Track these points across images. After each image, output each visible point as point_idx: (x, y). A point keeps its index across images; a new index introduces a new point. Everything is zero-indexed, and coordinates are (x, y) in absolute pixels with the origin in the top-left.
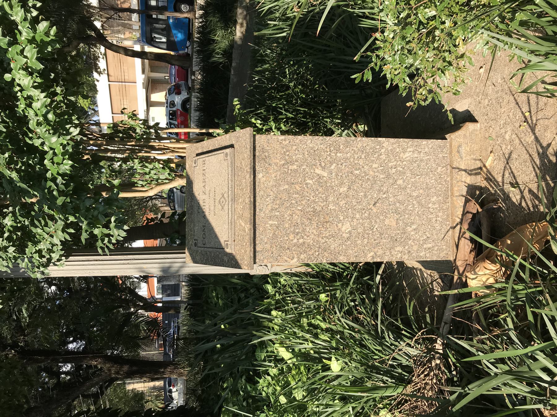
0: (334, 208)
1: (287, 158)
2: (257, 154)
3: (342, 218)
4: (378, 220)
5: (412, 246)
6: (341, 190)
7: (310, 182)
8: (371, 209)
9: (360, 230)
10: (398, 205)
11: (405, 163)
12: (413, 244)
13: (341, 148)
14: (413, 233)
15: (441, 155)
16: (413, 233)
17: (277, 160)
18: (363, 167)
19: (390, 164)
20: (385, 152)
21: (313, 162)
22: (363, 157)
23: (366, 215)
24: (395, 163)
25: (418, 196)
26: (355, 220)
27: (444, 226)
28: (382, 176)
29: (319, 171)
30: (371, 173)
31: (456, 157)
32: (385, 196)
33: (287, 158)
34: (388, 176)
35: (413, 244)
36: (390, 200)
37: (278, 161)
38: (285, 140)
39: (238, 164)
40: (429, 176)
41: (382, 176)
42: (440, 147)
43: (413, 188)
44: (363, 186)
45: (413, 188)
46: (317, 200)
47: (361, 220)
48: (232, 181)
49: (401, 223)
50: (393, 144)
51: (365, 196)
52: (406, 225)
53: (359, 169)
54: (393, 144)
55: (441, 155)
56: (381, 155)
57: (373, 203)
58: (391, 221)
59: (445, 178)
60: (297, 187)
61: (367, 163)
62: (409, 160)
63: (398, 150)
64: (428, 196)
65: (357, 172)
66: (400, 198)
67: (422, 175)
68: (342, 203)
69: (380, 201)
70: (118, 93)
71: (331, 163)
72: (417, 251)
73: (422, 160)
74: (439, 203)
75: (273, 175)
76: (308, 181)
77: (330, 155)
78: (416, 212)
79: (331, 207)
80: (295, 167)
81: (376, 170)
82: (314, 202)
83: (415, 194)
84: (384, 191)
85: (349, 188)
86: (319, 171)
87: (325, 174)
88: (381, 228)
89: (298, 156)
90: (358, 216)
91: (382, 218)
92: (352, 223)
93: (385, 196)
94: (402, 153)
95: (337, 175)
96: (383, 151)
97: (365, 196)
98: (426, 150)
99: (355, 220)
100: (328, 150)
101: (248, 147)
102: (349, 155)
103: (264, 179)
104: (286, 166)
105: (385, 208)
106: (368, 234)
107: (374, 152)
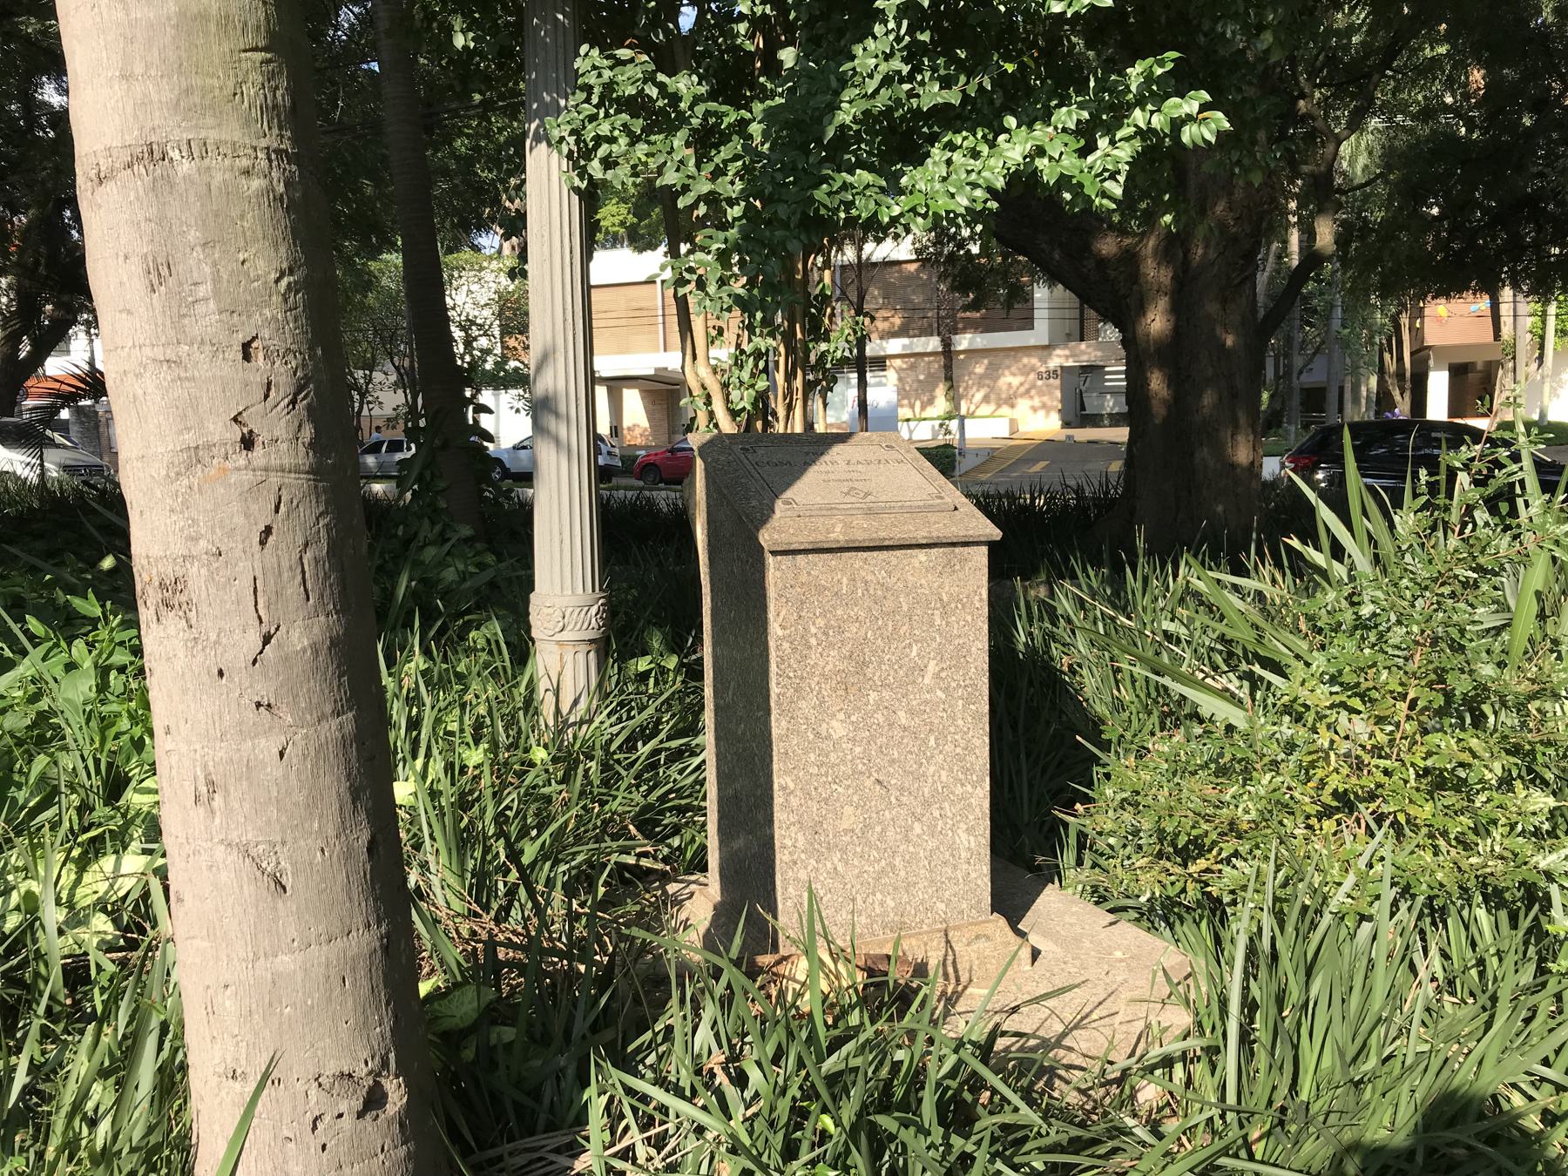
0: (871, 702)
1: (953, 605)
2: (957, 550)
3: (853, 718)
4: (850, 791)
5: (806, 868)
6: (901, 714)
7: (914, 653)
8: (871, 775)
9: (833, 756)
10: (878, 829)
11: (950, 834)
12: (810, 868)
13: (972, 707)
14: (829, 865)
15: (964, 906)
16: (829, 865)
17: (948, 588)
18: (941, 752)
19: (946, 805)
20: (967, 792)
21: (947, 656)
22: (958, 750)
23: (860, 766)
24: (949, 814)
25: (893, 867)
26: (850, 746)
27: (842, 930)
28: (926, 790)
29: (932, 667)
30: (932, 769)
31: (969, 934)
32: (894, 801)
33: (953, 605)
34: (927, 804)
35: (810, 868)
36: (887, 812)
37: (947, 589)
38: (981, 600)
39: (932, 518)
40: (929, 886)
41: (926, 790)
42: (979, 902)
43: (907, 857)
44: (909, 756)
45: (907, 857)
46: (883, 667)
47: (849, 757)
48: (901, 507)
49: (846, 839)
50: (981, 806)
51: (893, 761)
52: (844, 851)
53: (938, 745)
54: (981, 806)
55: (964, 906)
56: (963, 785)
57: (881, 779)
58: (850, 818)
59: (926, 921)
60: (905, 628)
61: (948, 759)
62: (954, 842)
63: (971, 817)
64: (895, 889)
65: (932, 742)
66: (890, 833)
67: (931, 871)
68: (879, 717)
69: (883, 792)
70: (635, 305)
71: (946, 690)
72: (797, 879)
73: (955, 867)
74: (885, 914)
75: (923, 581)
76: (915, 648)
77: (959, 686)
78: (866, 868)
79: (873, 696)
80: (938, 622)
81: (936, 778)
82: (881, 662)
83: (897, 861)
84: (902, 798)
85: (905, 729)
86: (932, 667)
87: (927, 681)
88: (837, 800)
89: (956, 626)
90: (858, 750)
91: (855, 798)
92: (845, 739)
93: (894, 801)
94: (965, 827)
95: (926, 702)
96: (969, 788)
97: (893, 761)
98: (973, 875)
99: (850, 746)
100: (967, 682)
101: (971, 533)
102: (960, 722)
103: (917, 565)
104: (938, 605)
105: (873, 803)
106: (826, 775)
107: (966, 771)
